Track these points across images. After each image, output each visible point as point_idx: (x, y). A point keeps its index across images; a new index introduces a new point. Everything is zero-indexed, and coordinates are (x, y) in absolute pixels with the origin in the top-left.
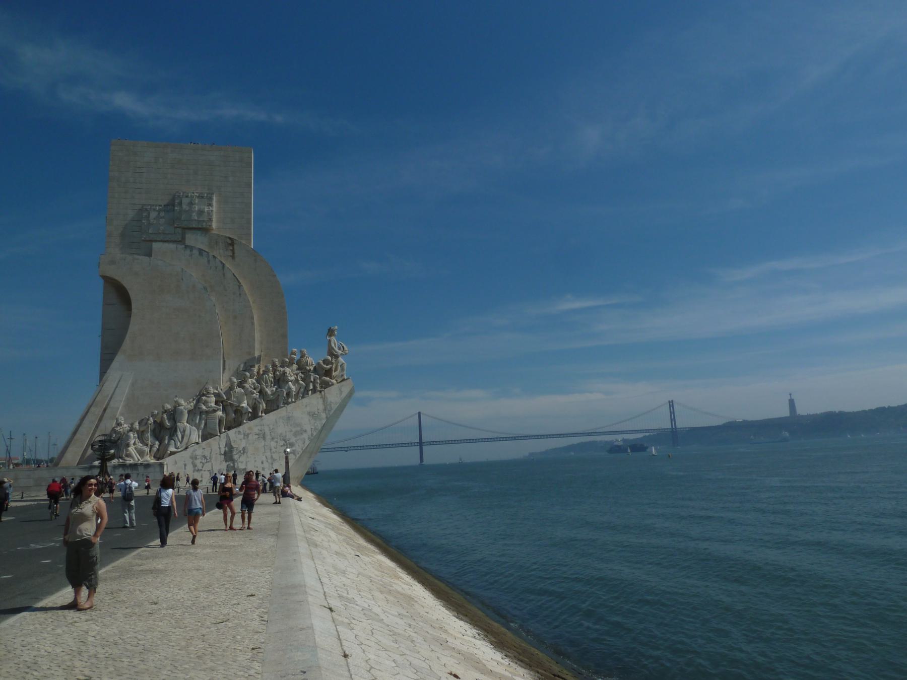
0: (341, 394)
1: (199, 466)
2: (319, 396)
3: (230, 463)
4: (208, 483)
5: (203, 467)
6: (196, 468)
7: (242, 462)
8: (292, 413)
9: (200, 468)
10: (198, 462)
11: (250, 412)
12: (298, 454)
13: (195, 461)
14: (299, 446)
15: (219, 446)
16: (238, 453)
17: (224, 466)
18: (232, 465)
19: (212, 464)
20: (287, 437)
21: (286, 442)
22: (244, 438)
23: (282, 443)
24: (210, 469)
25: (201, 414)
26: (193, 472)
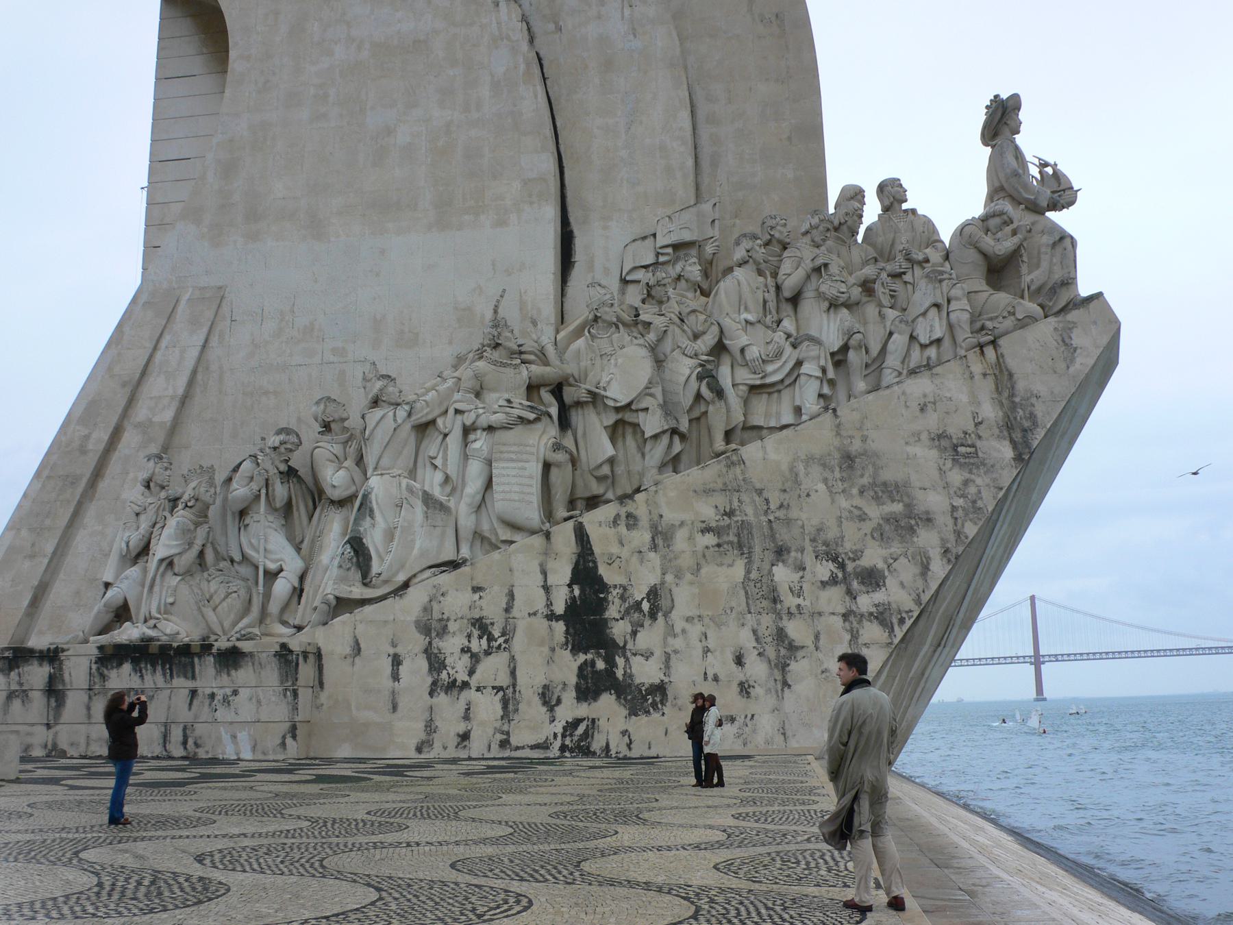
0: (1071, 361)
1: (458, 667)
2: (977, 368)
3: (589, 656)
4: (495, 746)
5: (471, 672)
6: (444, 675)
7: (648, 655)
8: (864, 439)
9: (462, 676)
10: (451, 645)
11: (674, 431)
12: (902, 621)
13: (437, 642)
14: (902, 584)
15: (546, 581)
16: (627, 612)
17: (568, 667)
18: (601, 665)
19: (513, 658)
20: (848, 546)
21: (842, 566)
22: (654, 547)
23: (825, 570)
24: (503, 680)
25: (472, 437)
26: (431, 694)
